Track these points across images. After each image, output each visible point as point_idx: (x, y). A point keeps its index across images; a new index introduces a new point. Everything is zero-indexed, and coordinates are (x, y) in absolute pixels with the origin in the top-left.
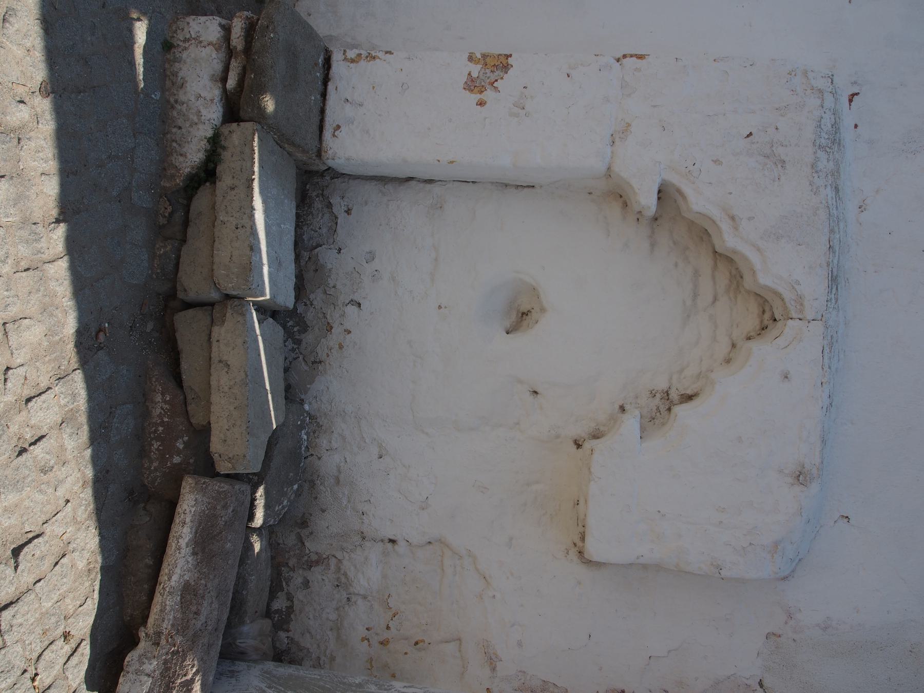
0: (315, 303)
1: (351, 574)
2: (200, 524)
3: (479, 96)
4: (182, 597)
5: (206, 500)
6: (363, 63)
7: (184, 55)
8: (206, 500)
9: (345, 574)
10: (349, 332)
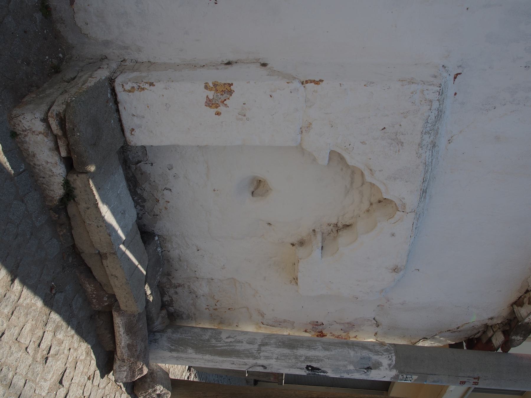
0: (146, 189)
2: (126, 325)
3: (216, 110)
7: (27, 139)
10: (169, 202)
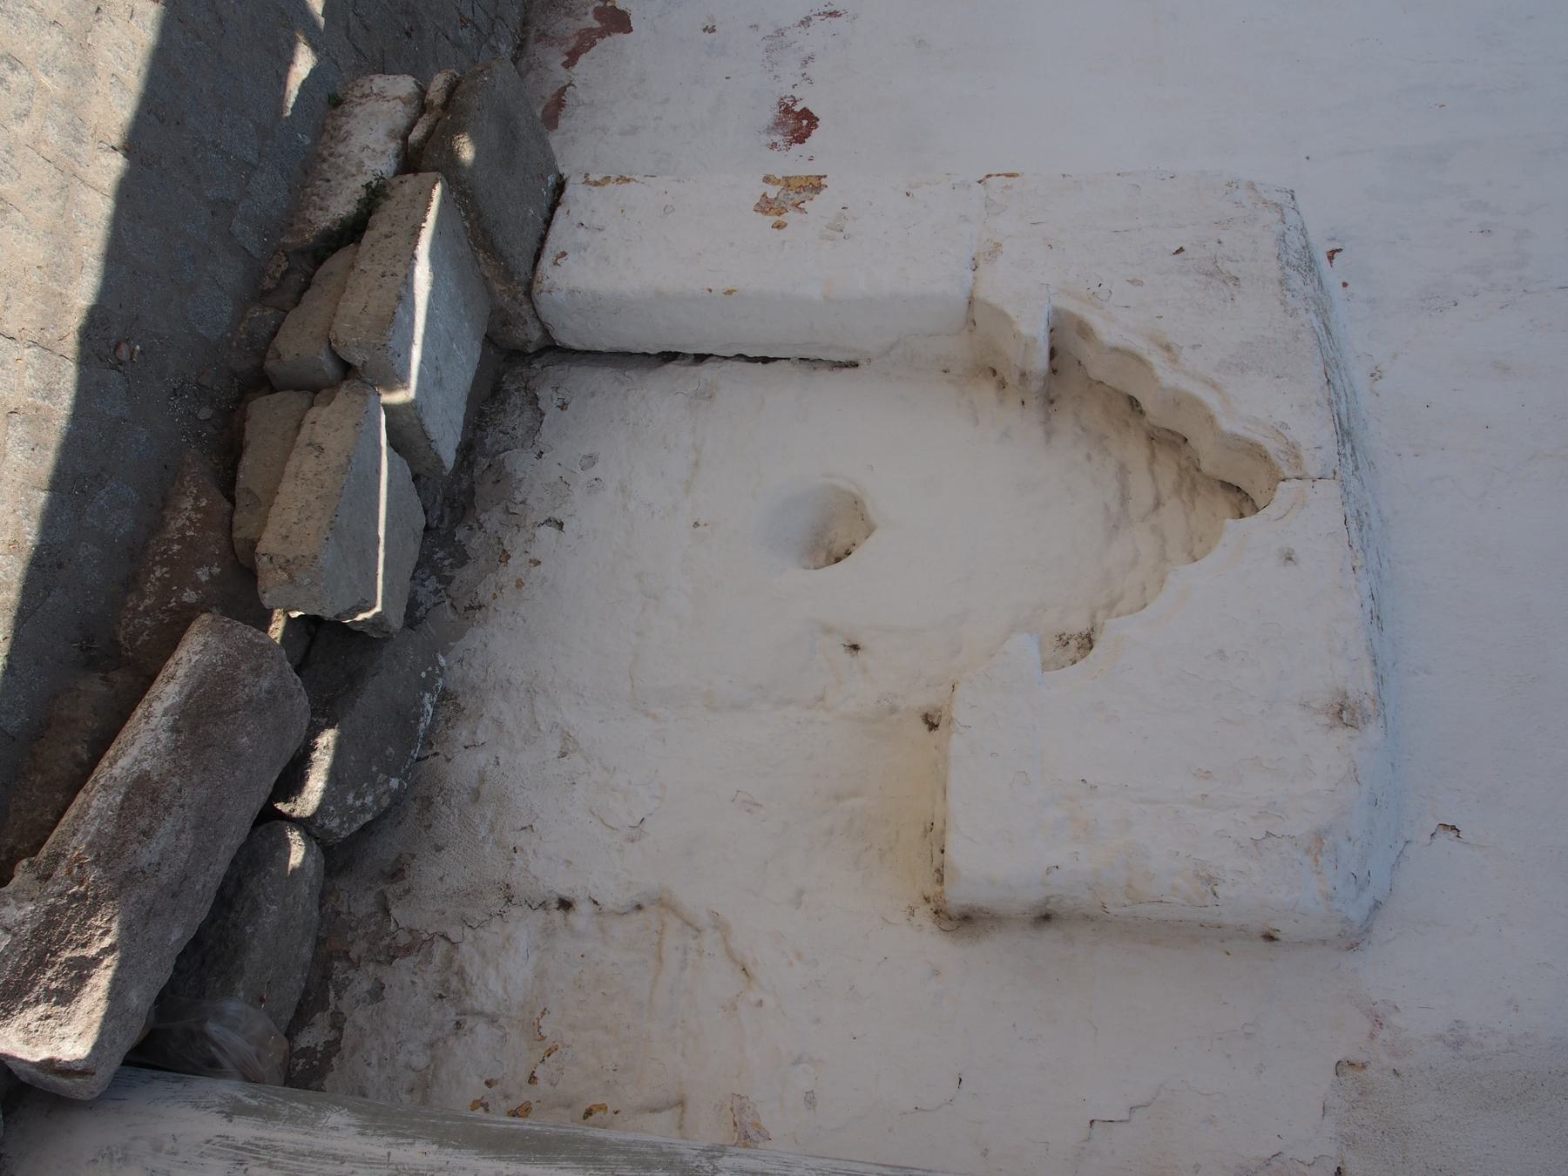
0: (487, 525)
1: (471, 972)
2: (201, 684)
3: (776, 218)
4: (127, 797)
5: (223, 648)
6: (611, 186)
7: (357, 110)
8: (223, 648)
9: (461, 973)
10: (538, 563)
